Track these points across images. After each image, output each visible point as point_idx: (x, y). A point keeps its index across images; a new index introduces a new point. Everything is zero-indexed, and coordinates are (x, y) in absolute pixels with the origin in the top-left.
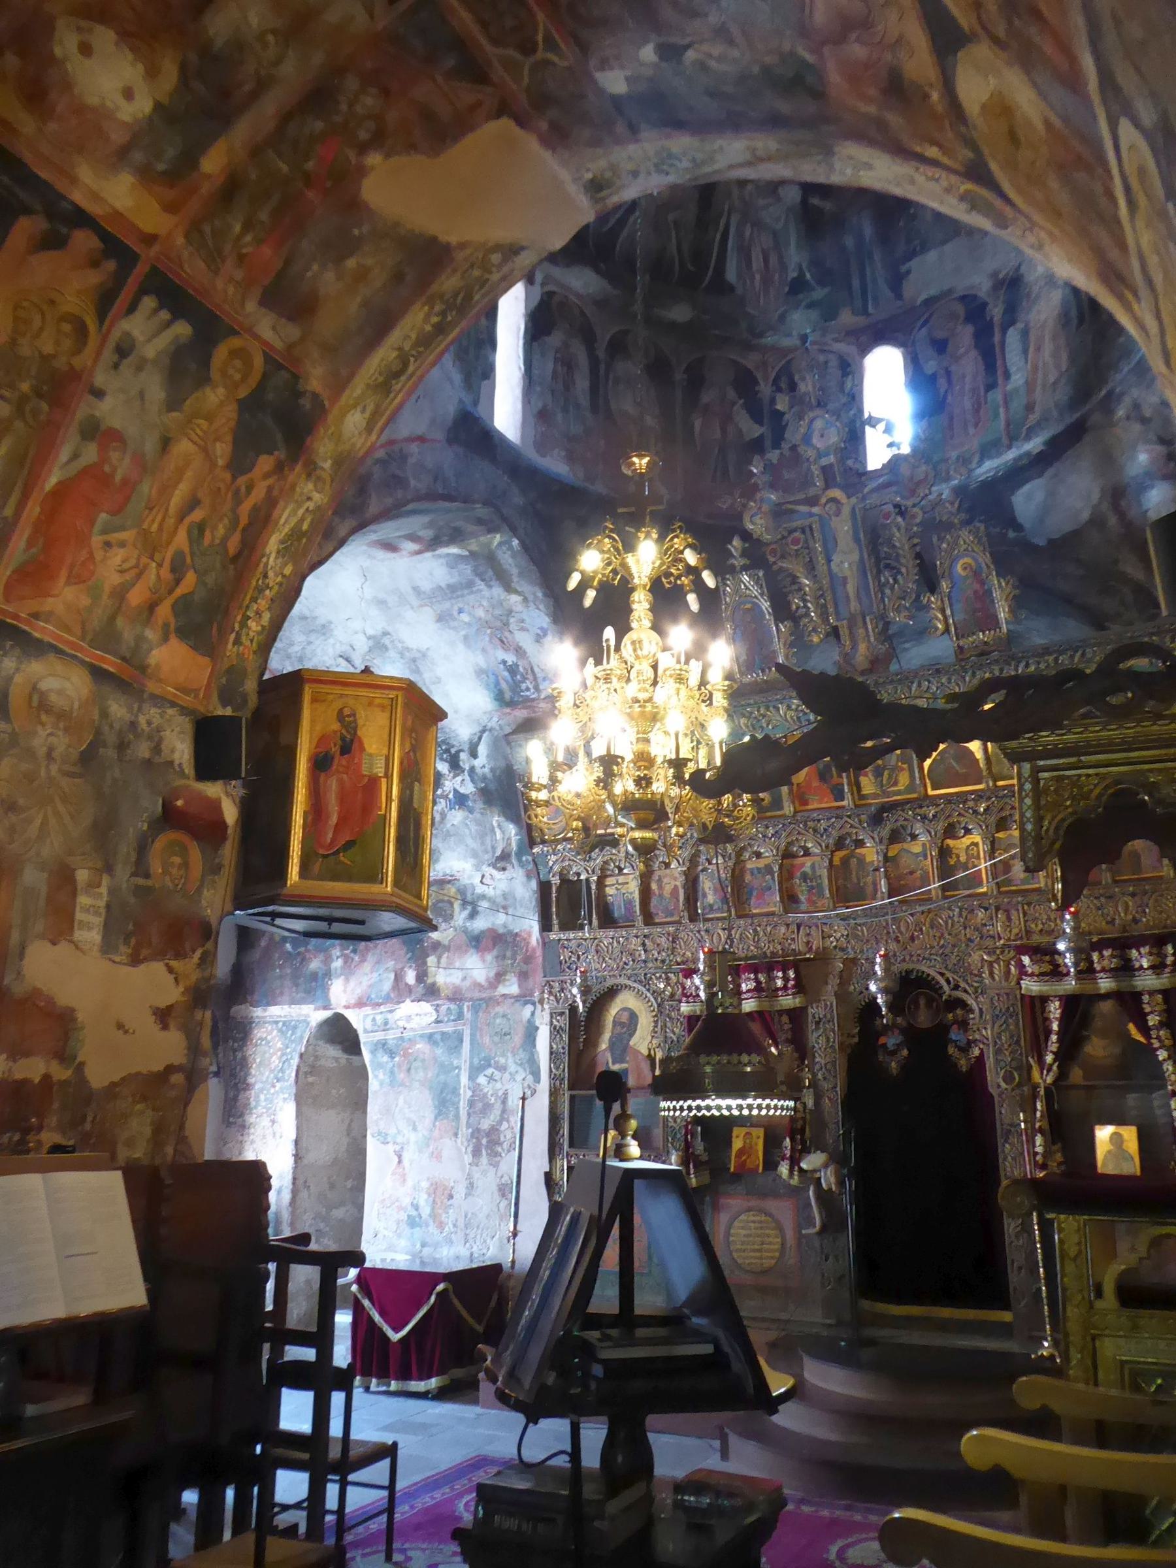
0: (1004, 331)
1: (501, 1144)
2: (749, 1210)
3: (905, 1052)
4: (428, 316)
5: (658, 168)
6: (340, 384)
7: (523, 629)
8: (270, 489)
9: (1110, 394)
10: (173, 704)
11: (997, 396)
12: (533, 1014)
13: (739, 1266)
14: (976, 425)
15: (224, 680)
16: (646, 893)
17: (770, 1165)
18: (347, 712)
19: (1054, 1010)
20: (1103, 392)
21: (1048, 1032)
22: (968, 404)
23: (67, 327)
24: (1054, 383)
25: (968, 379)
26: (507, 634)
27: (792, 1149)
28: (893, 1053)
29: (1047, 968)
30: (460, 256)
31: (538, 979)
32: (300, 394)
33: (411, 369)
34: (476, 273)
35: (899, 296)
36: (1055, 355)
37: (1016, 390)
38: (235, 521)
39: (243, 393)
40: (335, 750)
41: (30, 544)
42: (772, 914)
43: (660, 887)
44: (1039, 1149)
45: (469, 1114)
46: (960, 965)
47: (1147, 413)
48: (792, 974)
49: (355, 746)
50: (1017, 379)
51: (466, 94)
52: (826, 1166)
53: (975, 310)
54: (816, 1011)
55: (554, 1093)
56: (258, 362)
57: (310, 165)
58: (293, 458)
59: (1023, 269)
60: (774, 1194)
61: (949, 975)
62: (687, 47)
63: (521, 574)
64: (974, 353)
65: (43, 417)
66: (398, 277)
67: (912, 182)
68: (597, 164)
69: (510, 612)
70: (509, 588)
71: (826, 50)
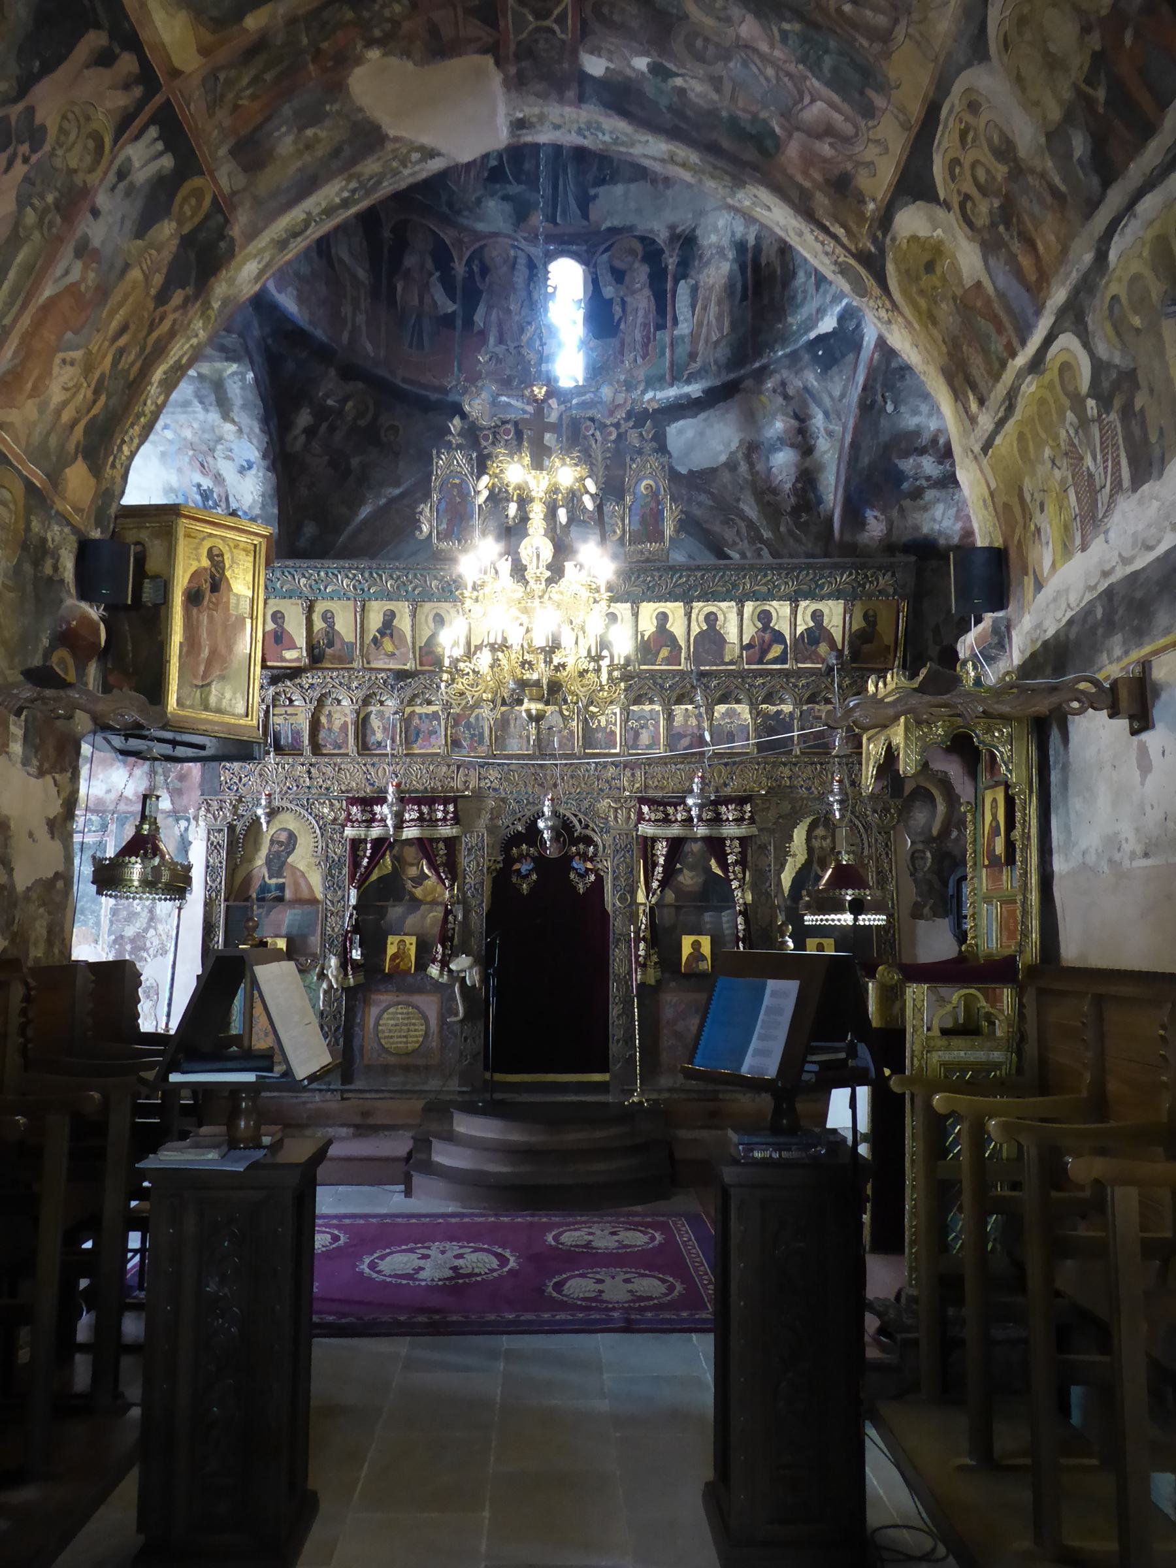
0: (676, 283)
1: (146, 950)
2: (399, 1003)
3: (534, 877)
4: (342, 190)
5: (580, 132)
6: (253, 234)
7: (228, 458)
8: (175, 321)
9: (764, 368)
10: (69, 523)
11: (664, 336)
12: (187, 829)
13: (386, 1051)
14: (644, 358)
15: (100, 502)
16: (315, 725)
17: (422, 966)
18: (215, 552)
19: (661, 849)
20: (757, 365)
21: (655, 865)
22: (638, 336)
23: (91, 144)
24: (717, 343)
25: (641, 313)
26: (210, 459)
27: (444, 955)
28: (527, 876)
29: (660, 816)
30: (390, 146)
31: (195, 795)
32: (222, 237)
33: (309, 232)
34: (395, 164)
35: (585, 215)
36: (719, 318)
37: (682, 337)
38: (143, 349)
39: (186, 230)
40: (206, 587)
41: (16, 353)
42: (438, 754)
43: (330, 721)
44: (642, 953)
45: (111, 922)
46: (591, 811)
47: (791, 391)
48: (451, 808)
49: (223, 586)
50: (684, 328)
51: (474, 29)
52: (471, 968)
53: (652, 254)
54: (468, 840)
55: (209, 904)
56: (207, 202)
57: (325, 45)
58: (196, 297)
59: (698, 232)
60: (420, 990)
61: (581, 816)
62: (677, 75)
63: (244, 407)
64: (647, 292)
65: (54, 230)
66: (336, 152)
67: (801, 234)
68: (529, 110)
69: (220, 439)
70: (226, 416)
71: (796, 134)
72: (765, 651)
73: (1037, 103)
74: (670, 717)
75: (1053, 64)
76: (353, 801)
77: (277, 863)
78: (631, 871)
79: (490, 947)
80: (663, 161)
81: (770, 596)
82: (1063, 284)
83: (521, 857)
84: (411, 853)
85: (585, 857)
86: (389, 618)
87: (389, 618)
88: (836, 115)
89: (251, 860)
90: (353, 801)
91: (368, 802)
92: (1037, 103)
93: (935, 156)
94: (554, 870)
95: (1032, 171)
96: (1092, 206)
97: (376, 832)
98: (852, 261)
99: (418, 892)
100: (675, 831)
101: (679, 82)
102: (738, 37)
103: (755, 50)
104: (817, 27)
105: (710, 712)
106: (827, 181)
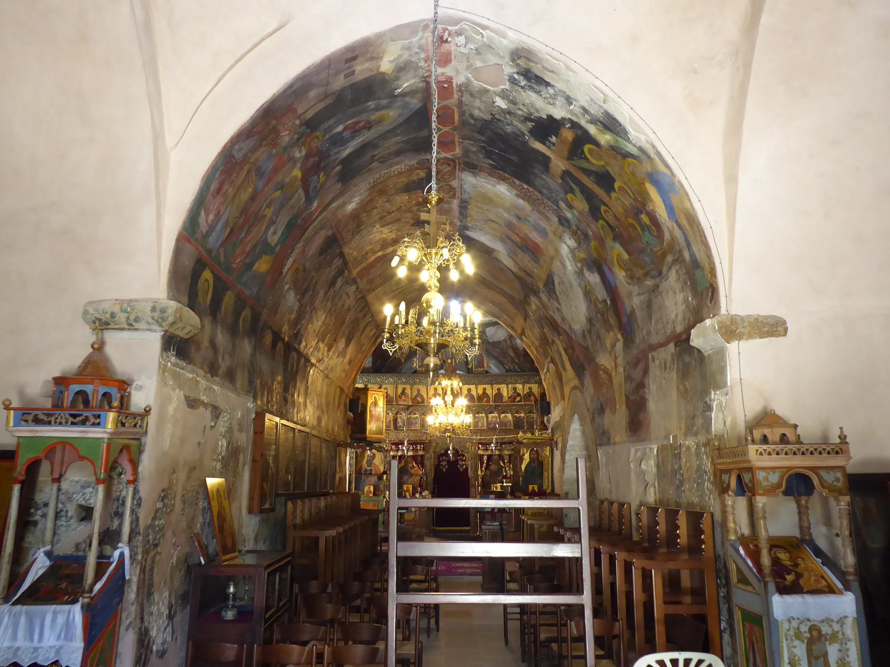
19: (485, 458)
46: (464, 447)
54: (427, 456)
72: (515, 399)
74: (487, 418)
76: (393, 444)
77: (370, 463)
78: (476, 465)
79: (434, 488)
81: (516, 383)
83: (443, 460)
84: (410, 460)
85: (462, 460)
86: (404, 389)
87: (404, 389)
89: (361, 462)
90: (393, 444)
91: (398, 444)
94: (453, 465)
97: (400, 453)
99: (412, 471)
100: (489, 453)
105: (499, 416)
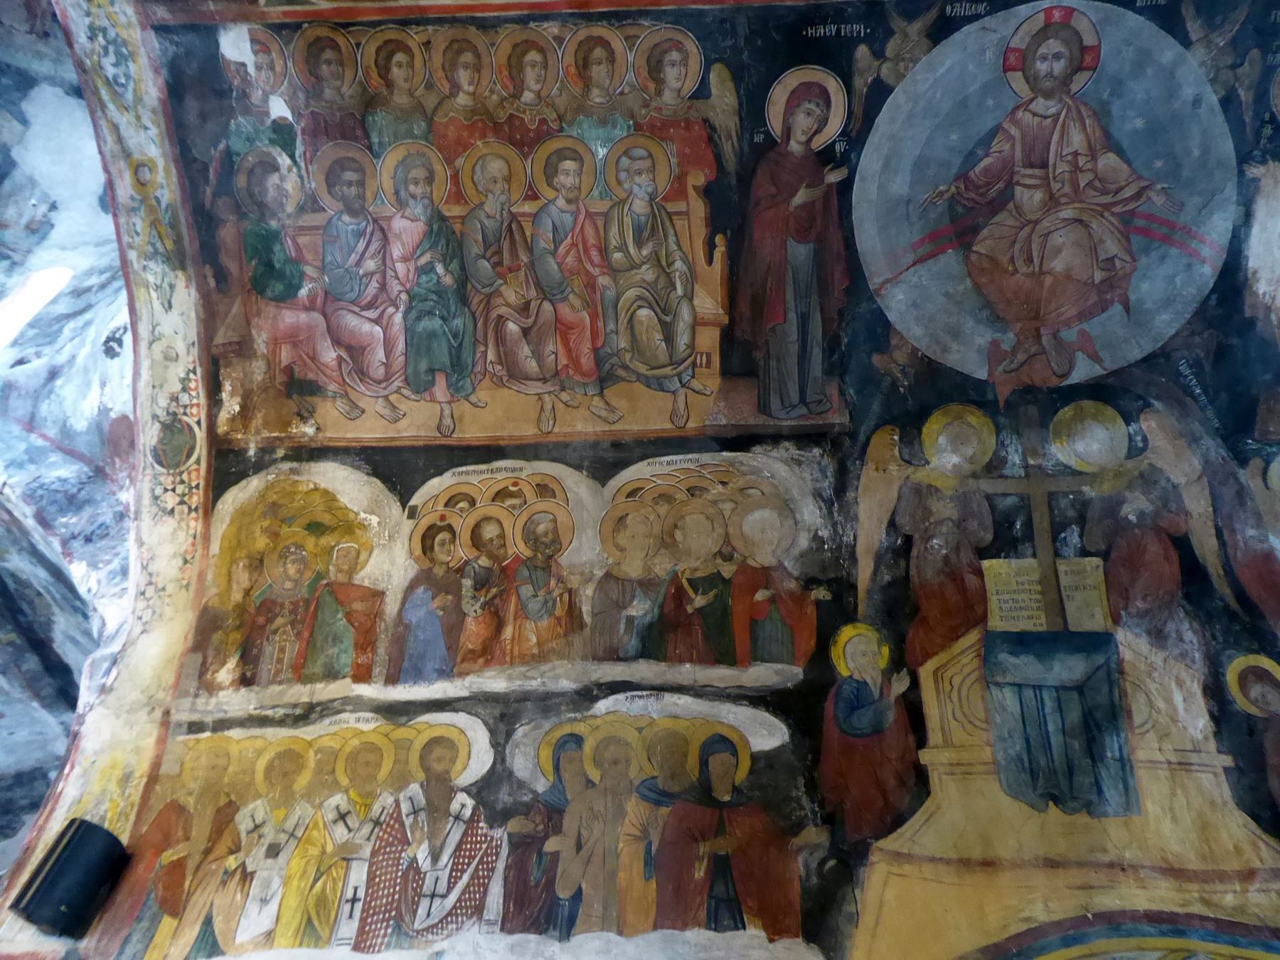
62: (292, 157)
73: (622, 550)
75: (667, 541)
80: (127, 154)
82: (510, 678)
88: (380, 355)
92: (622, 550)
93: (448, 474)
95: (560, 580)
96: (614, 655)
98: (200, 435)
101: (284, 160)
102: (390, 218)
103: (385, 239)
104: (464, 300)
106: (289, 370)
